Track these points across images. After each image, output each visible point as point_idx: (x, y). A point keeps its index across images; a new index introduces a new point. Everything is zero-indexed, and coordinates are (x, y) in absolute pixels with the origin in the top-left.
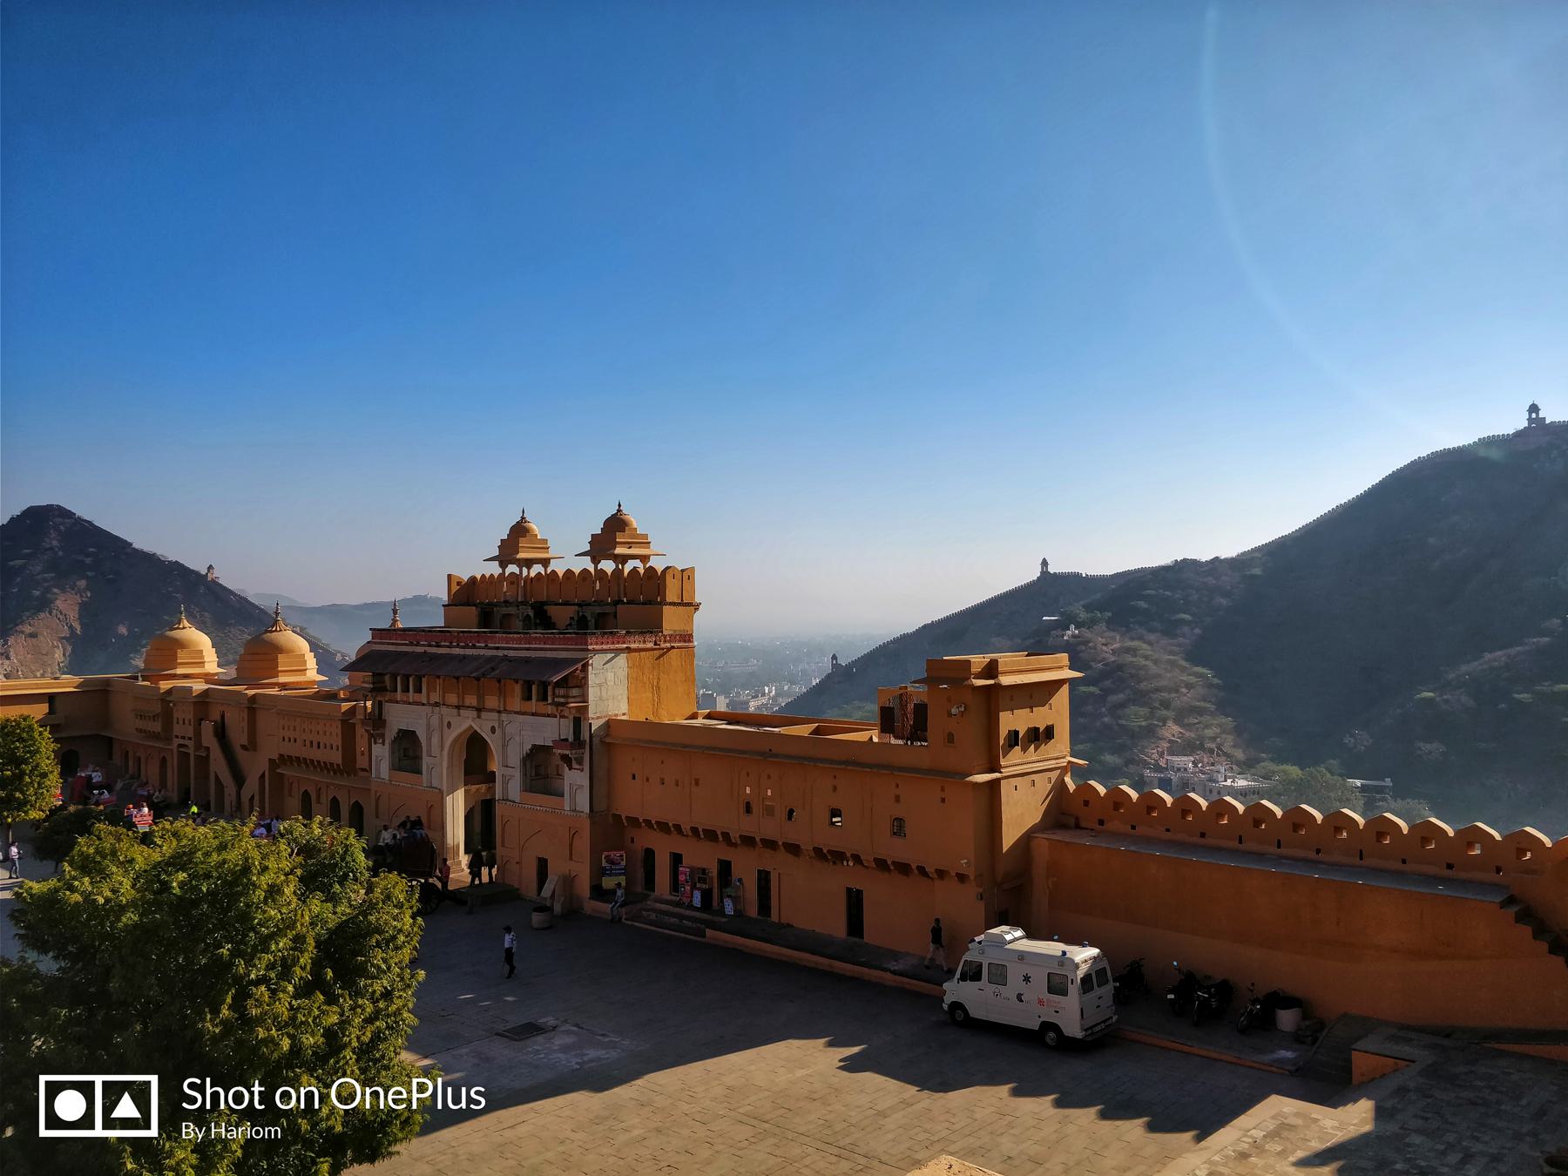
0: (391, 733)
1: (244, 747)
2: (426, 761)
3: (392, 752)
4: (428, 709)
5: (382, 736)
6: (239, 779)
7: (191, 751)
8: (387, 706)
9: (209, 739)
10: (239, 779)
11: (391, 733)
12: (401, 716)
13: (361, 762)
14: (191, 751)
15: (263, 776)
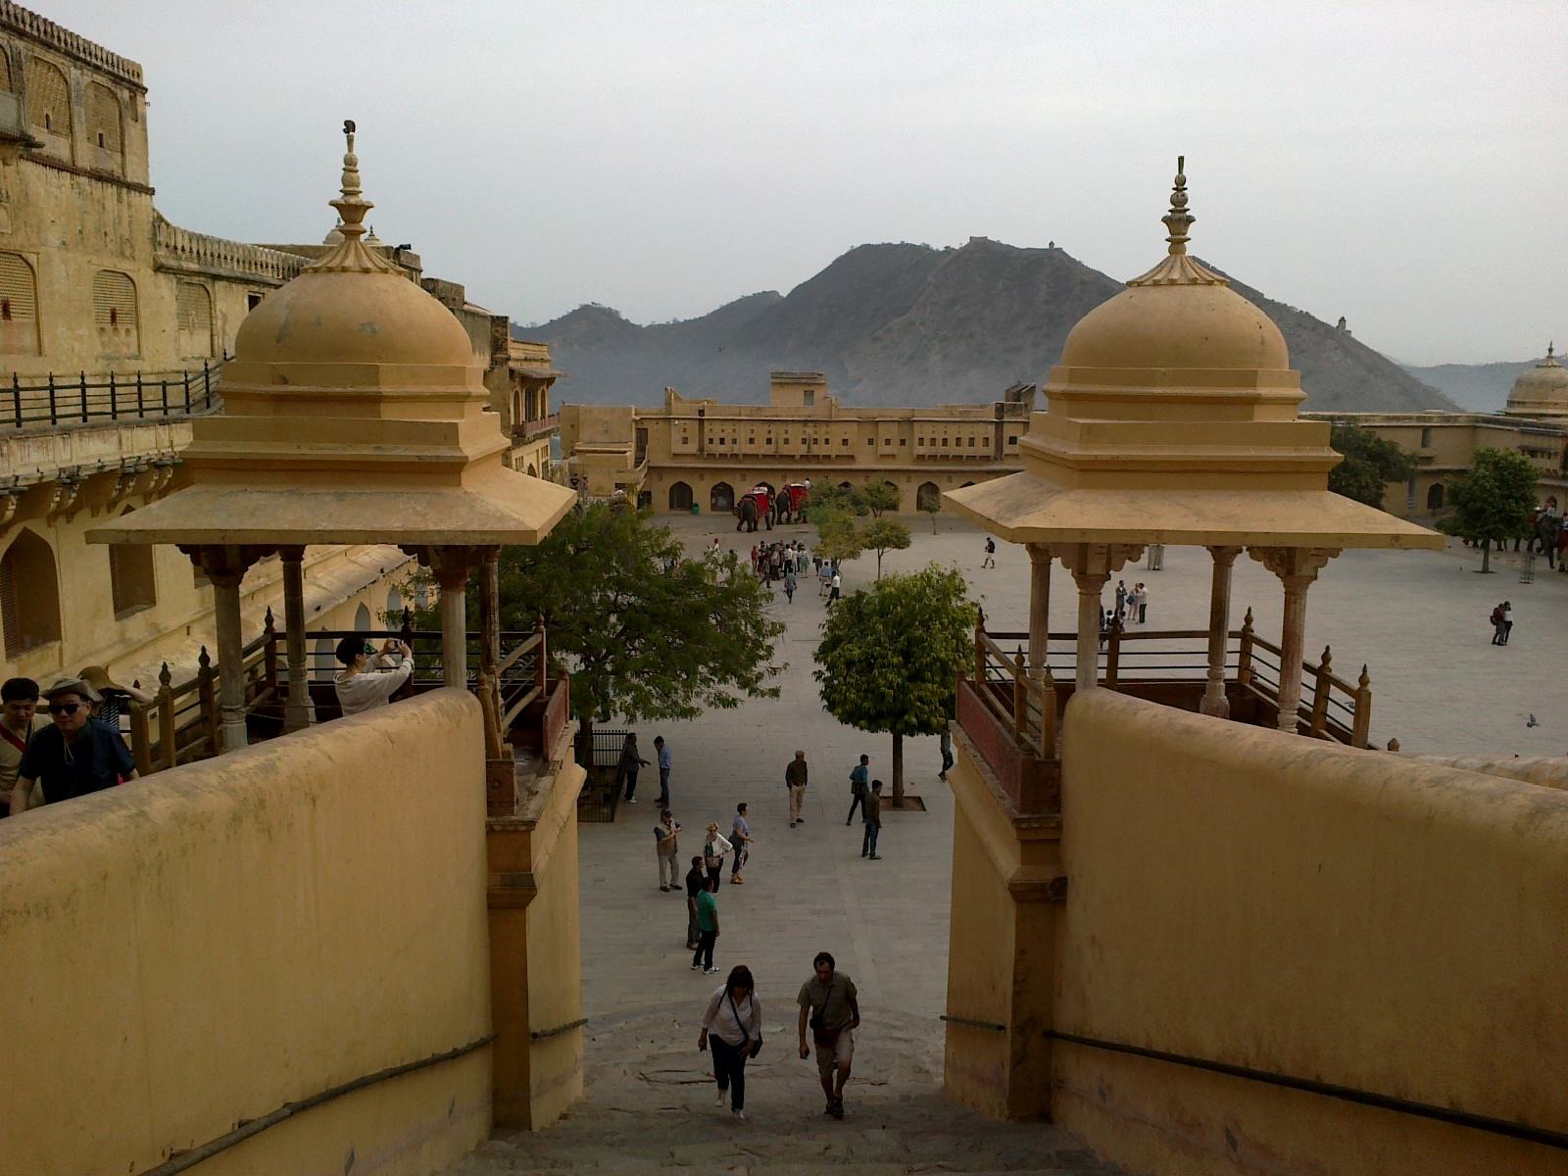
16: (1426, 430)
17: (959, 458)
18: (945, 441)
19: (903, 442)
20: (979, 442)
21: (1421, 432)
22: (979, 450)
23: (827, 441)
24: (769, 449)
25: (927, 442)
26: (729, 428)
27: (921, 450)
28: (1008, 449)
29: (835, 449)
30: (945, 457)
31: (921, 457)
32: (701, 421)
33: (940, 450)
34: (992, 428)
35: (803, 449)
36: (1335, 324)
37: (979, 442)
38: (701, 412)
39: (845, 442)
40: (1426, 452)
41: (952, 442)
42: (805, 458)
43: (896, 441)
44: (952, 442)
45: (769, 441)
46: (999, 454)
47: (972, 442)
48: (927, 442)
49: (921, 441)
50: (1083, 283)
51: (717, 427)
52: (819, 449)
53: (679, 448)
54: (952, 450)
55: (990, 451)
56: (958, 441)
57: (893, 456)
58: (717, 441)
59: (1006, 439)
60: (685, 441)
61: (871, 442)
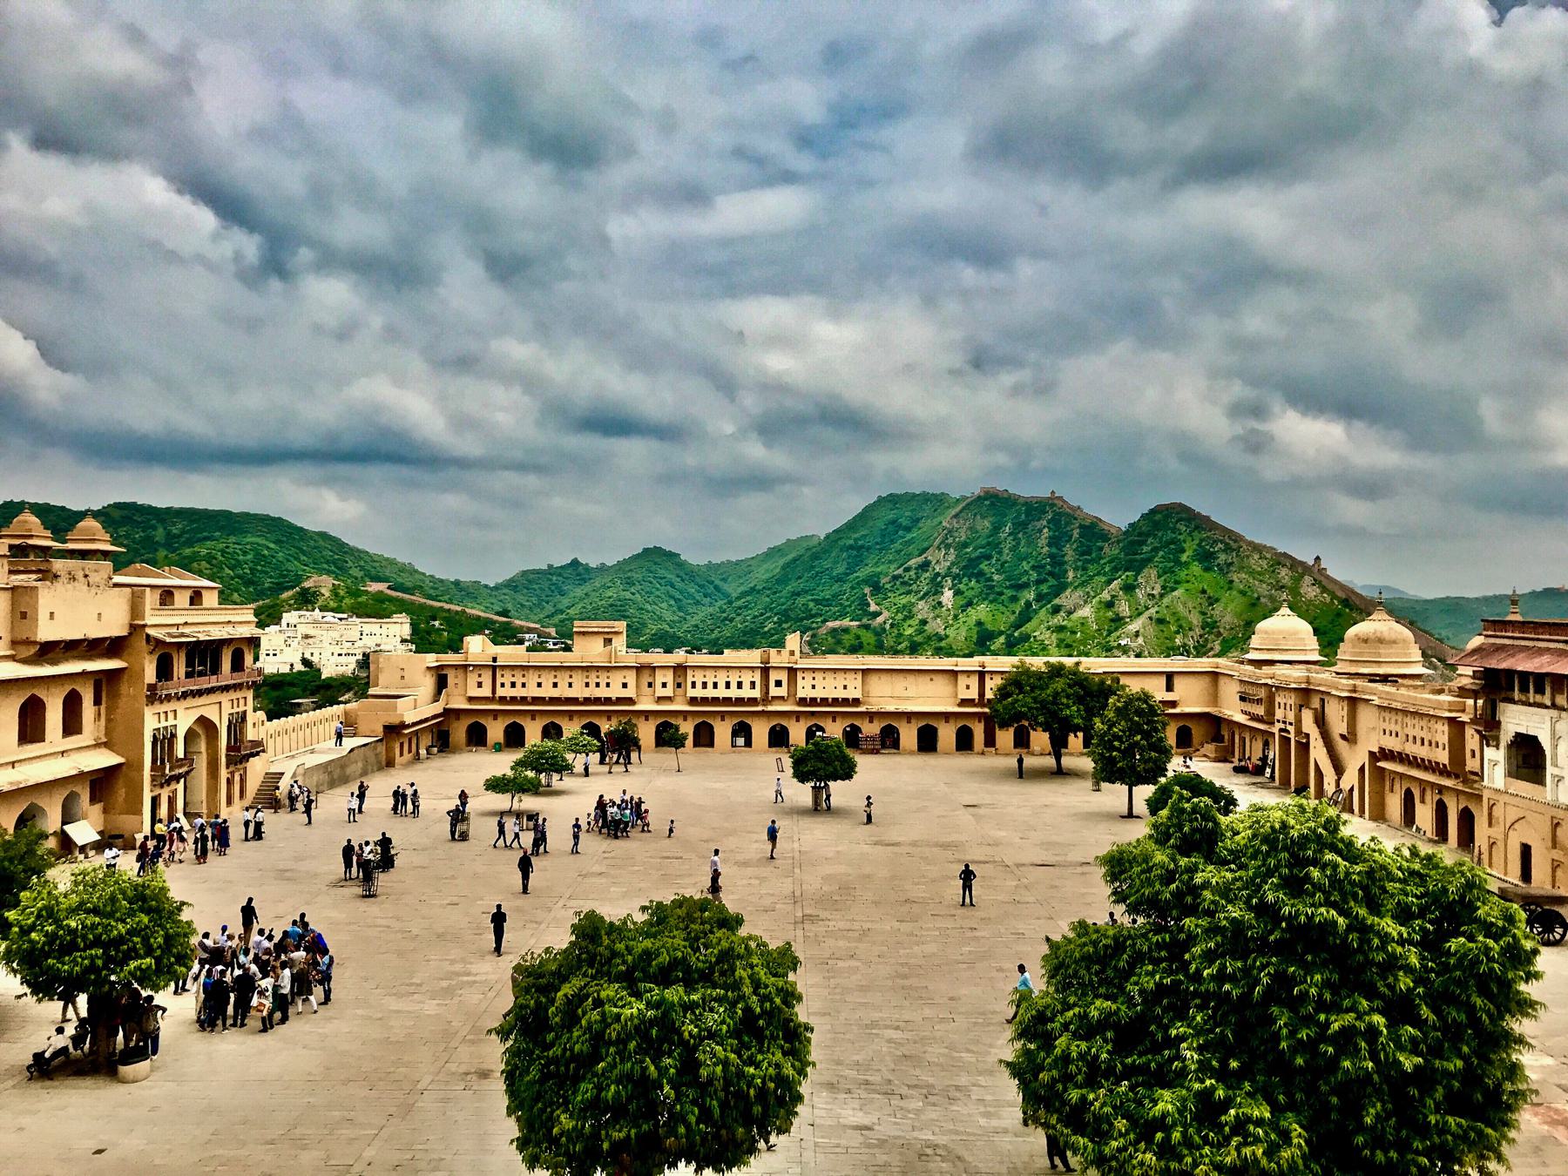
0: (1506, 736)
1: (1343, 737)
2: (1550, 770)
3: (1509, 758)
4: (1554, 713)
5: (1497, 739)
6: (1339, 770)
7: (1292, 736)
8: (1502, 706)
9: (1309, 725)
10: (1339, 770)
11: (1506, 736)
12: (1517, 719)
13: (1472, 764)
14: (1292, 736)
15: (1362, 770)
16: (1170, 677)
17: (727, 701)
18: (715, 685)
19: (679, 686)
20: (746, 685)
21: (1163, 680)
22: (746, 693)
23: (608, 685)
24: (555, 693)
25: (699, 685)
26: (518, 674)
27: (691, 693)
28: (774, 691)
29: (616, 692)
30: (715, 701)
31: (693, 701)
32: (494, 669)
33: (710, 693)
34: (757, 677)
35: (587, 693)
36: (1311, 562)
37: (746, 685)
38: (495, 660)
39: (625, 685)
40: (1169, 697)
41: (722, 685)
42: (587, 701)
43: (670, 685)
44: (722, 685)
45: (555, 685)
46: (766, 699)
47: (740, 685)
48: (699, 685)
49: (694, 685)
50: (1081, 527)
51: (508, 673)
52: (602, 693)
53: (474, 692)
54: (722, 693)
55: (756, 693)
56: (715, 685)
57: (669, 699)
58: (508, 685)
59: (772, 684)
60: (480, 685)
61: (650, 685)
